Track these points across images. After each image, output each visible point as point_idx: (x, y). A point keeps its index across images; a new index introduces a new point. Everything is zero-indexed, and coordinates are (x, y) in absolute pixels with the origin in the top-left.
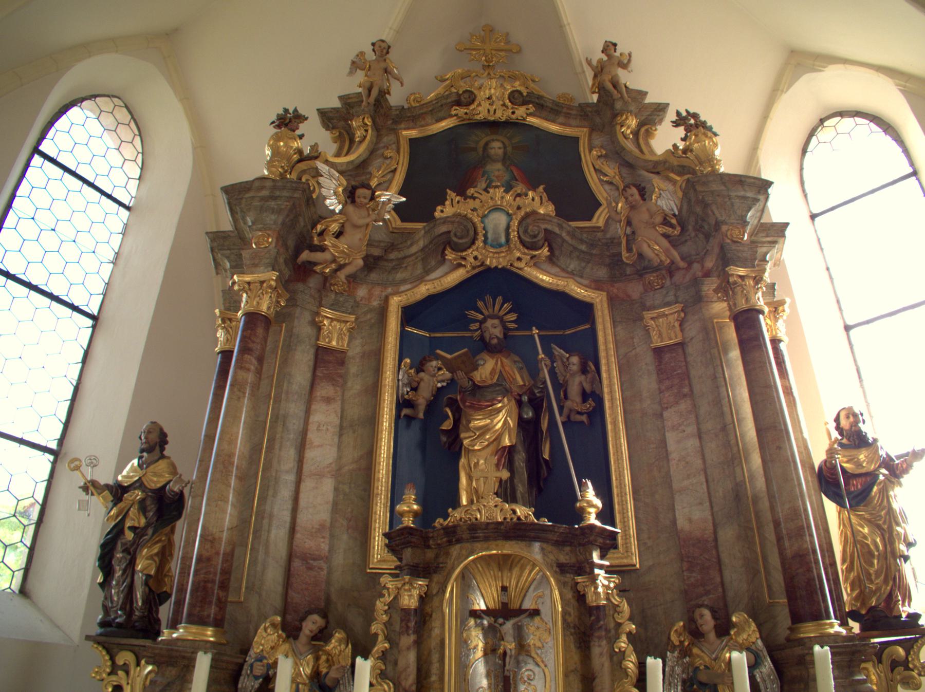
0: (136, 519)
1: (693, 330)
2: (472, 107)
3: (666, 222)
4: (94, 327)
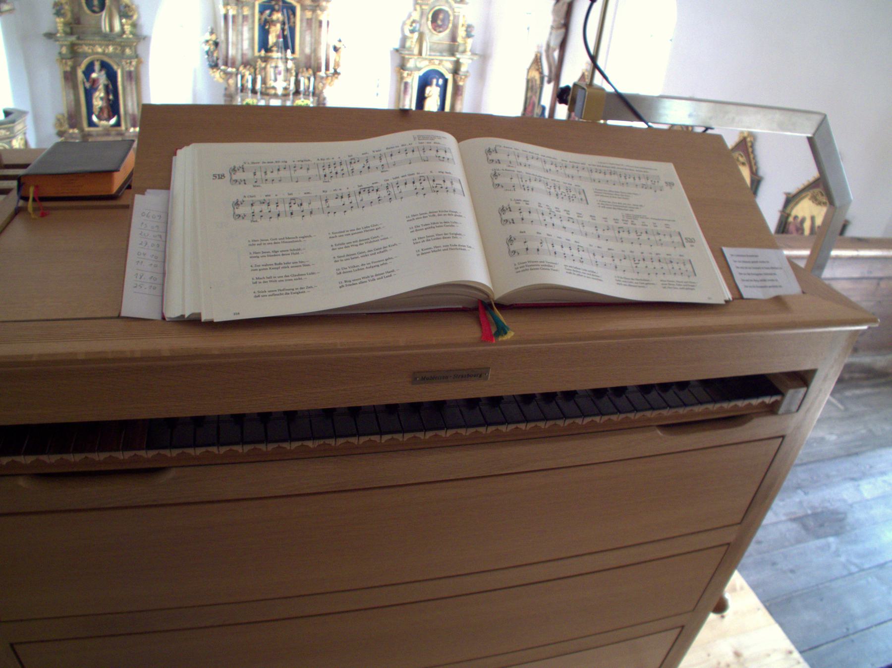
0: (213, 47)
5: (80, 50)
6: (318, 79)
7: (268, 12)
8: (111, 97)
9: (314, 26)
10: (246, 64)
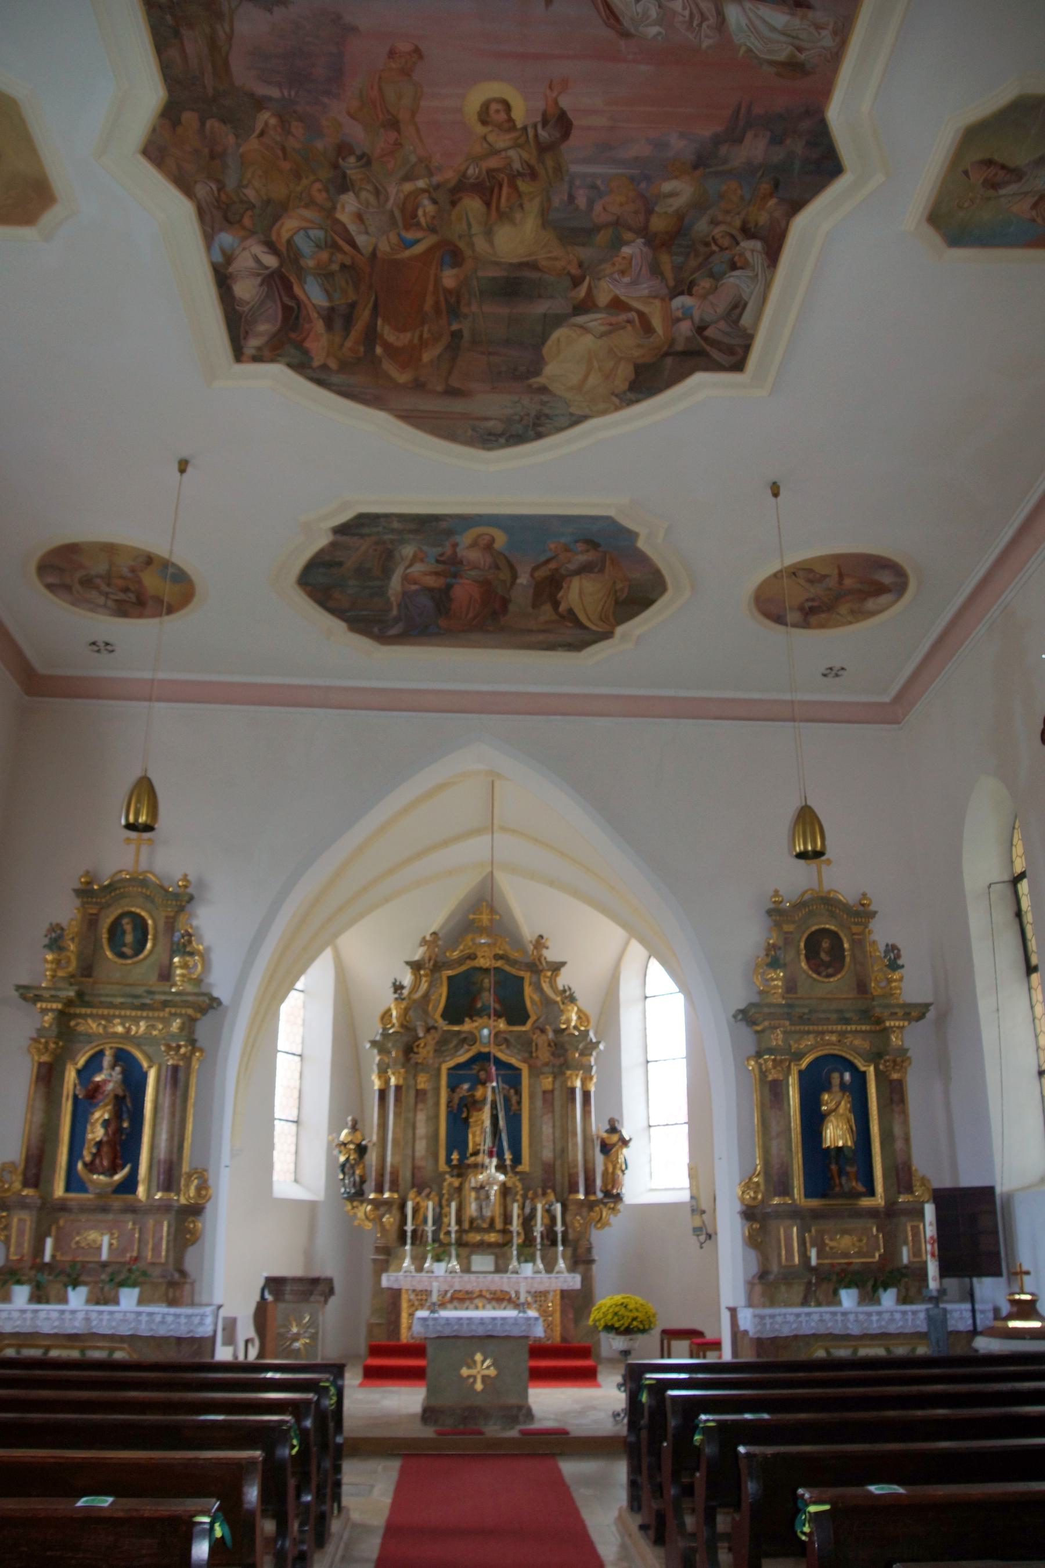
1: (557, 1085)
2: (476, 961)
3: (549, 1045)
4: (302, 1060)
5: (81, 1028)
6: (572, 1208)
7: (466, 1086)
8: (125, 1125)
9: (558, 1104)
10: (419, 1185)
